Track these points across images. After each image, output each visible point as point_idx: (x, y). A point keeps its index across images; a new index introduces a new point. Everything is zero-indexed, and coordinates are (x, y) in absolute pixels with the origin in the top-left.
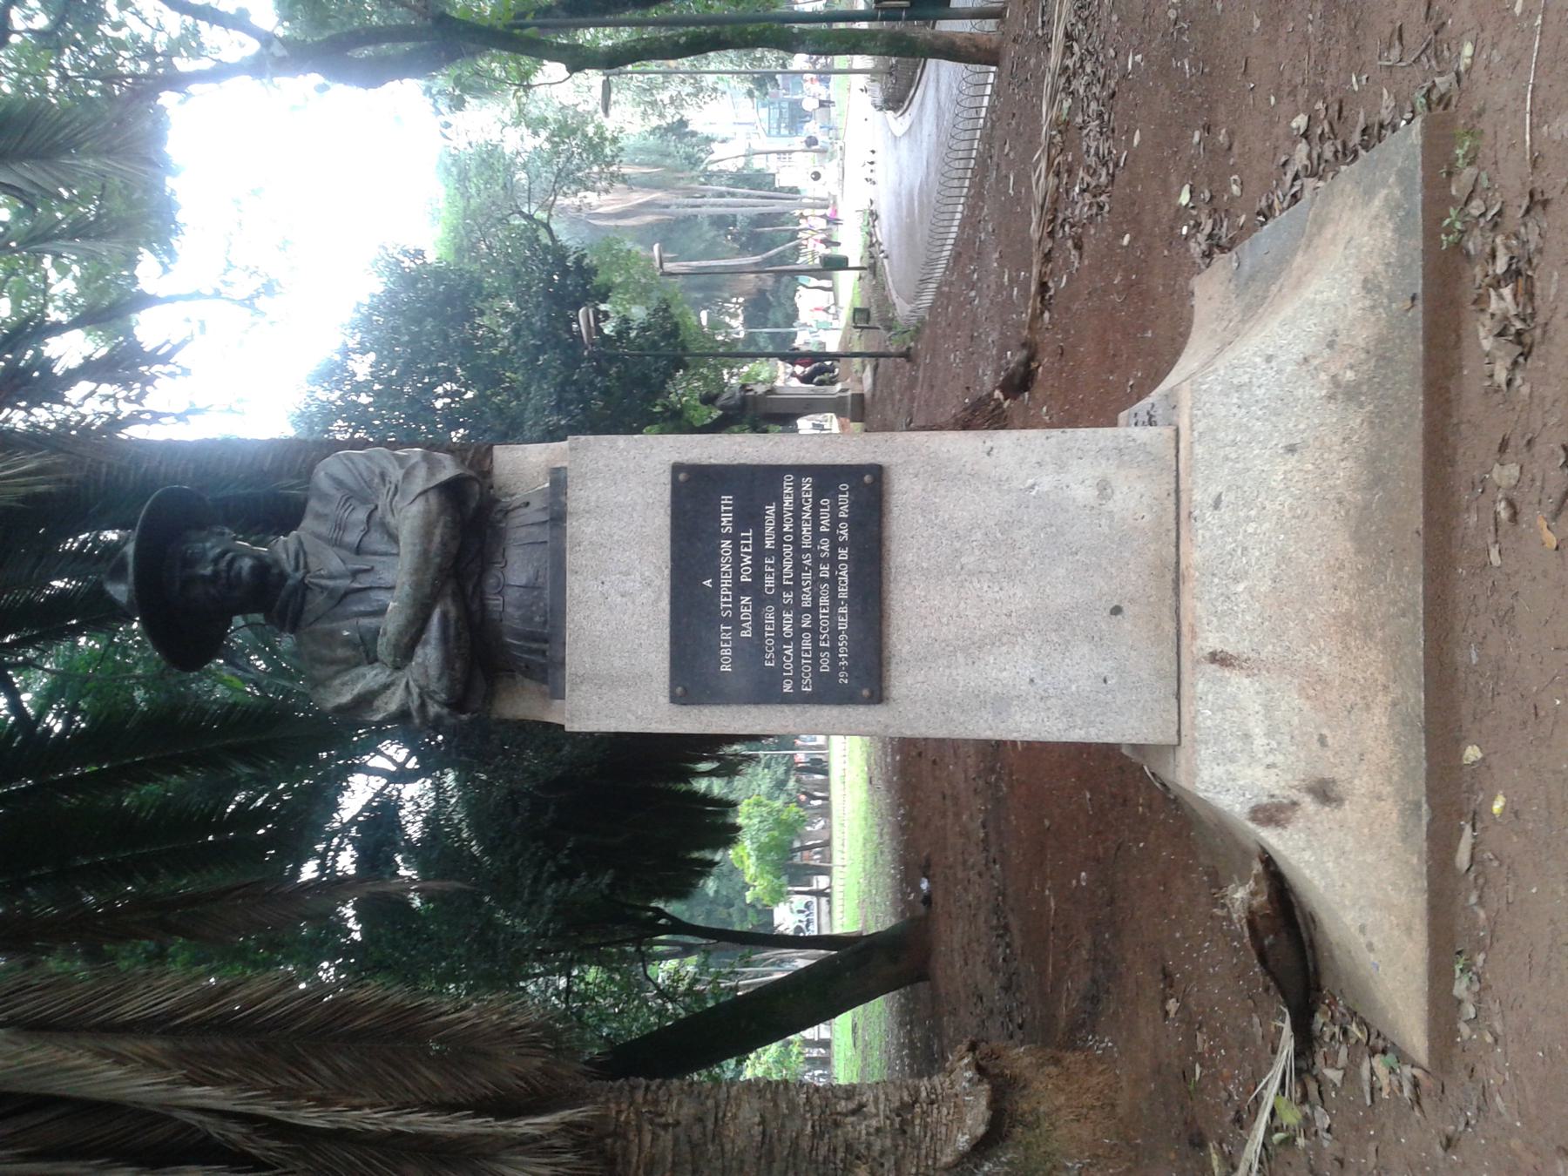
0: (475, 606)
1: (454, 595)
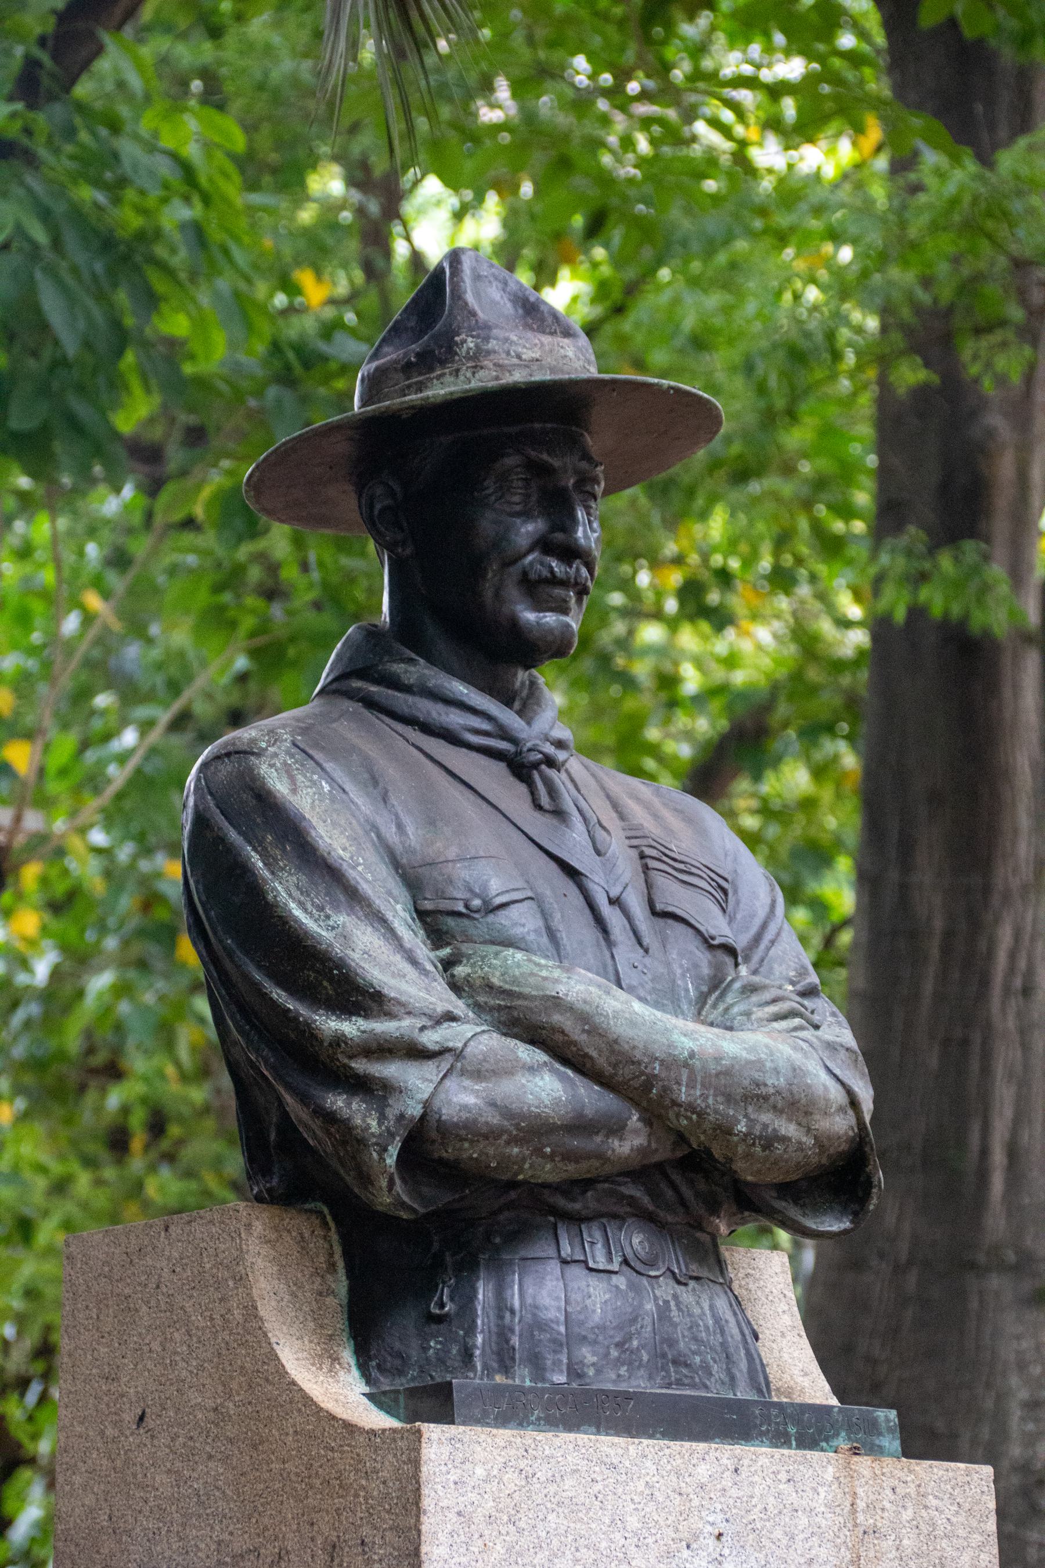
0: (589, 1201)
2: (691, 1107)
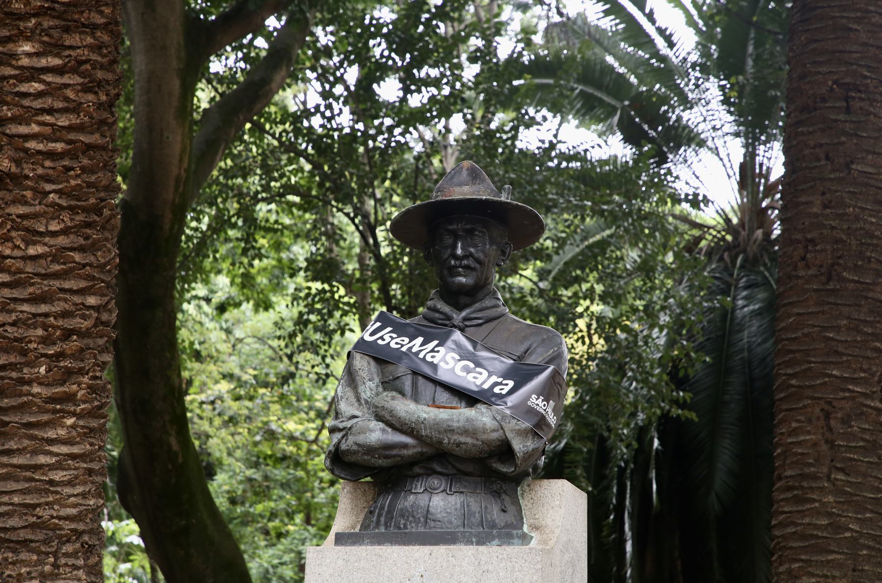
0: (417, 470)
1: (422, 454)
2: (427, 436)
